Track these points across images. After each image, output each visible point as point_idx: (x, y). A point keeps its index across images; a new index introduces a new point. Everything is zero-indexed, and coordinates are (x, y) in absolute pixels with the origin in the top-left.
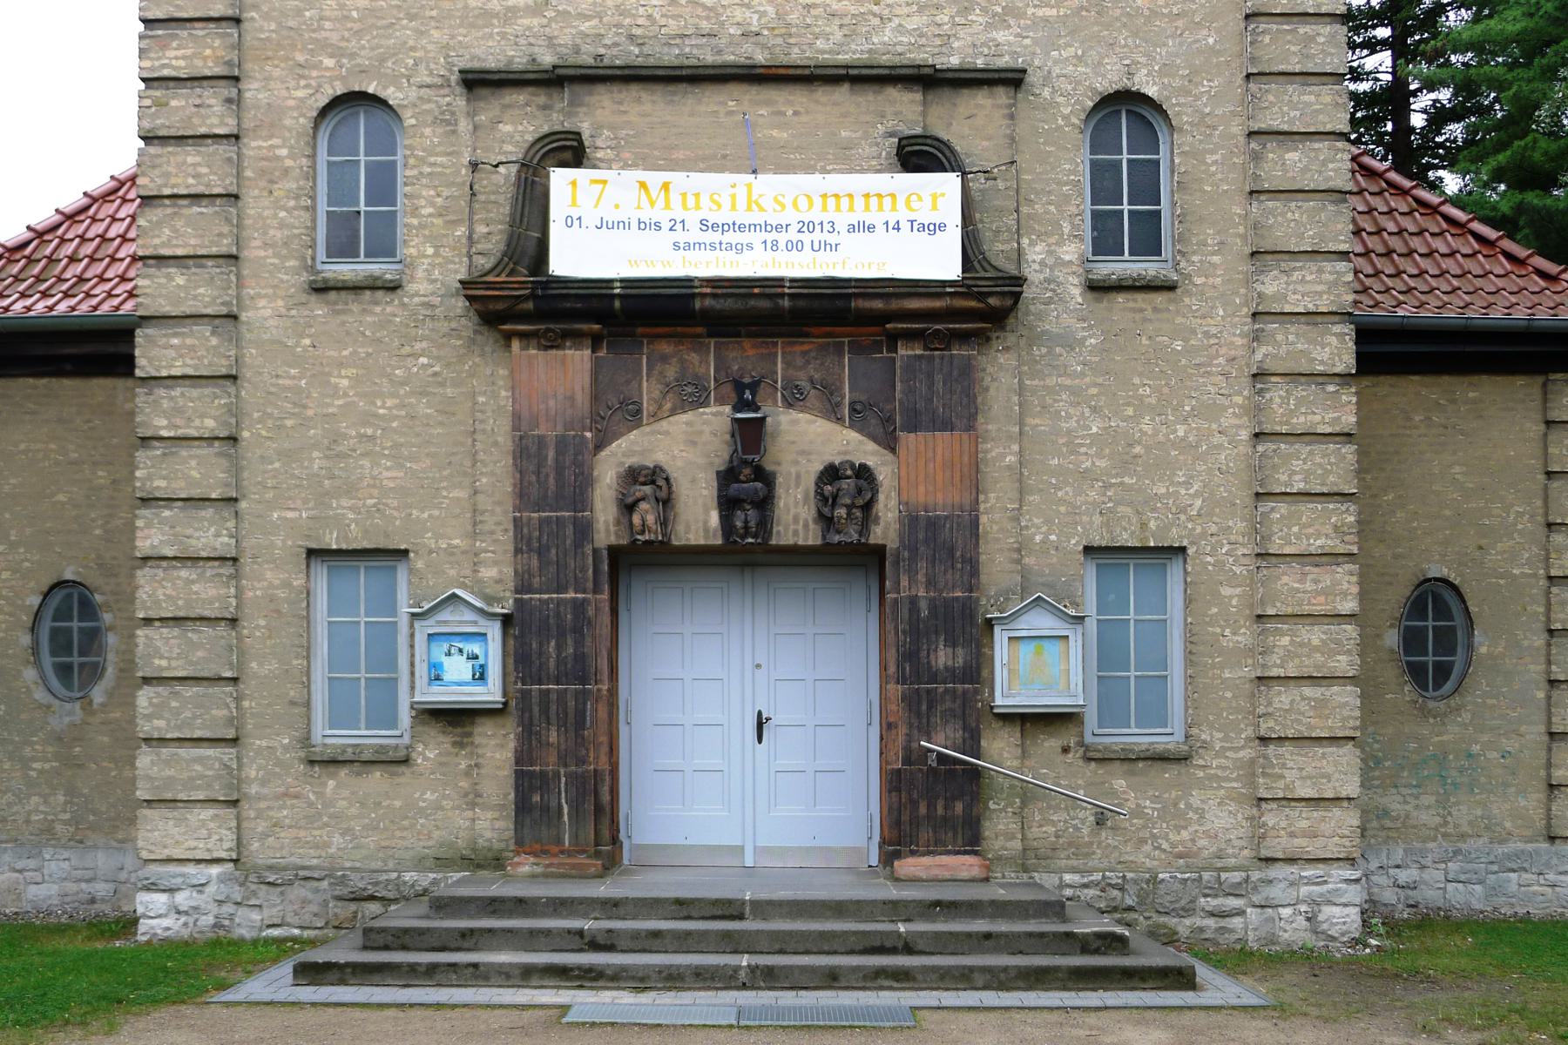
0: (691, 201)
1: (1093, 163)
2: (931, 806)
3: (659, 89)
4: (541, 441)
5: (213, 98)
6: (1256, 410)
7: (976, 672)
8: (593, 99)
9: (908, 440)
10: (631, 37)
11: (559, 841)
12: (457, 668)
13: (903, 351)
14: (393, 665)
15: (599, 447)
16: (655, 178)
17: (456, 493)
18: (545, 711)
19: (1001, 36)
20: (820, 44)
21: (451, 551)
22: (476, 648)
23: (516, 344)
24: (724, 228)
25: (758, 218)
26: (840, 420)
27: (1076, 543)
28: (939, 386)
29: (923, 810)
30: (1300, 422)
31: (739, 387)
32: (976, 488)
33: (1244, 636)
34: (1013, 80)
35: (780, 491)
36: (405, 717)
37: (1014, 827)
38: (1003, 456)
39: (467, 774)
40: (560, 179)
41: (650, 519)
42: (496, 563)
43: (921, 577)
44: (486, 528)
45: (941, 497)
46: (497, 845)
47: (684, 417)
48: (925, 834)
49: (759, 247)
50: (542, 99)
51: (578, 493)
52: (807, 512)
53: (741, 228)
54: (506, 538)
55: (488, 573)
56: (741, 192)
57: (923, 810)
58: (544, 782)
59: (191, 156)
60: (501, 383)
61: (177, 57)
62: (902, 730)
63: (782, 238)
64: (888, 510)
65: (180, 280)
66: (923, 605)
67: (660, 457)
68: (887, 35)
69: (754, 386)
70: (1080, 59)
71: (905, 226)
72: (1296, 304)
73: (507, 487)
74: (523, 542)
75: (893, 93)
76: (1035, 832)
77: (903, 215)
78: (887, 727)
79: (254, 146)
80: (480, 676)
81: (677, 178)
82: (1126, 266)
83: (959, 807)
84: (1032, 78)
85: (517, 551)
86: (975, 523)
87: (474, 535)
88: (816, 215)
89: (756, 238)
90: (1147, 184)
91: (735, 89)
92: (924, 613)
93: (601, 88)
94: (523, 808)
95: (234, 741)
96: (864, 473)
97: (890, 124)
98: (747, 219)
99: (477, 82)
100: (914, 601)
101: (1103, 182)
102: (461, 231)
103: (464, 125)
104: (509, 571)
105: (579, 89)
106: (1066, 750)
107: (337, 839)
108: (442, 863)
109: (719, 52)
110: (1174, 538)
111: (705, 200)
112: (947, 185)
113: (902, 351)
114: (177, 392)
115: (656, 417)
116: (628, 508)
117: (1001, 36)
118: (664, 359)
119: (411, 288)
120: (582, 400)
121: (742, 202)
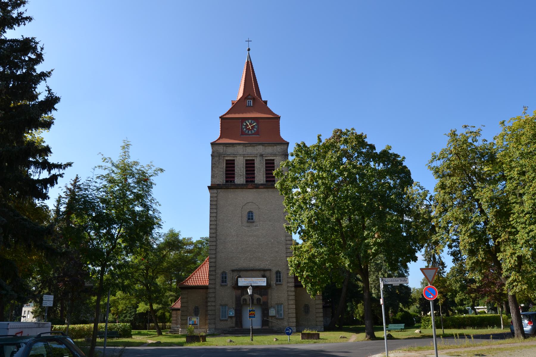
5: (214, 272)
6: (288, 294)
7: (268, 313)
9: (263, 296)
12: (231, 313)
13: (263, 290)
14: (226, 313)
16: (245, 278)
19: (269, 267)
30: (291, 294)
33: (287, 310)
34: (270, 270)
36: (227, 317)
40: (239, 279)
52: (256, 302)
59: (212, 276)
61: (212, 269)
64: (262, 301)
72: (290, 286)
79: (217, 275)
80: (233, 314)
82: (279, 283)
90: (280, 277)
94: (236, 323)
96: (260, 299)
99: (233, 271)
101: (277, 277)
103: (232, 274)
108: (230, 328)
110: (282, 303)
112: (265, 279)
116: (243, 302)
117: (269, 267)
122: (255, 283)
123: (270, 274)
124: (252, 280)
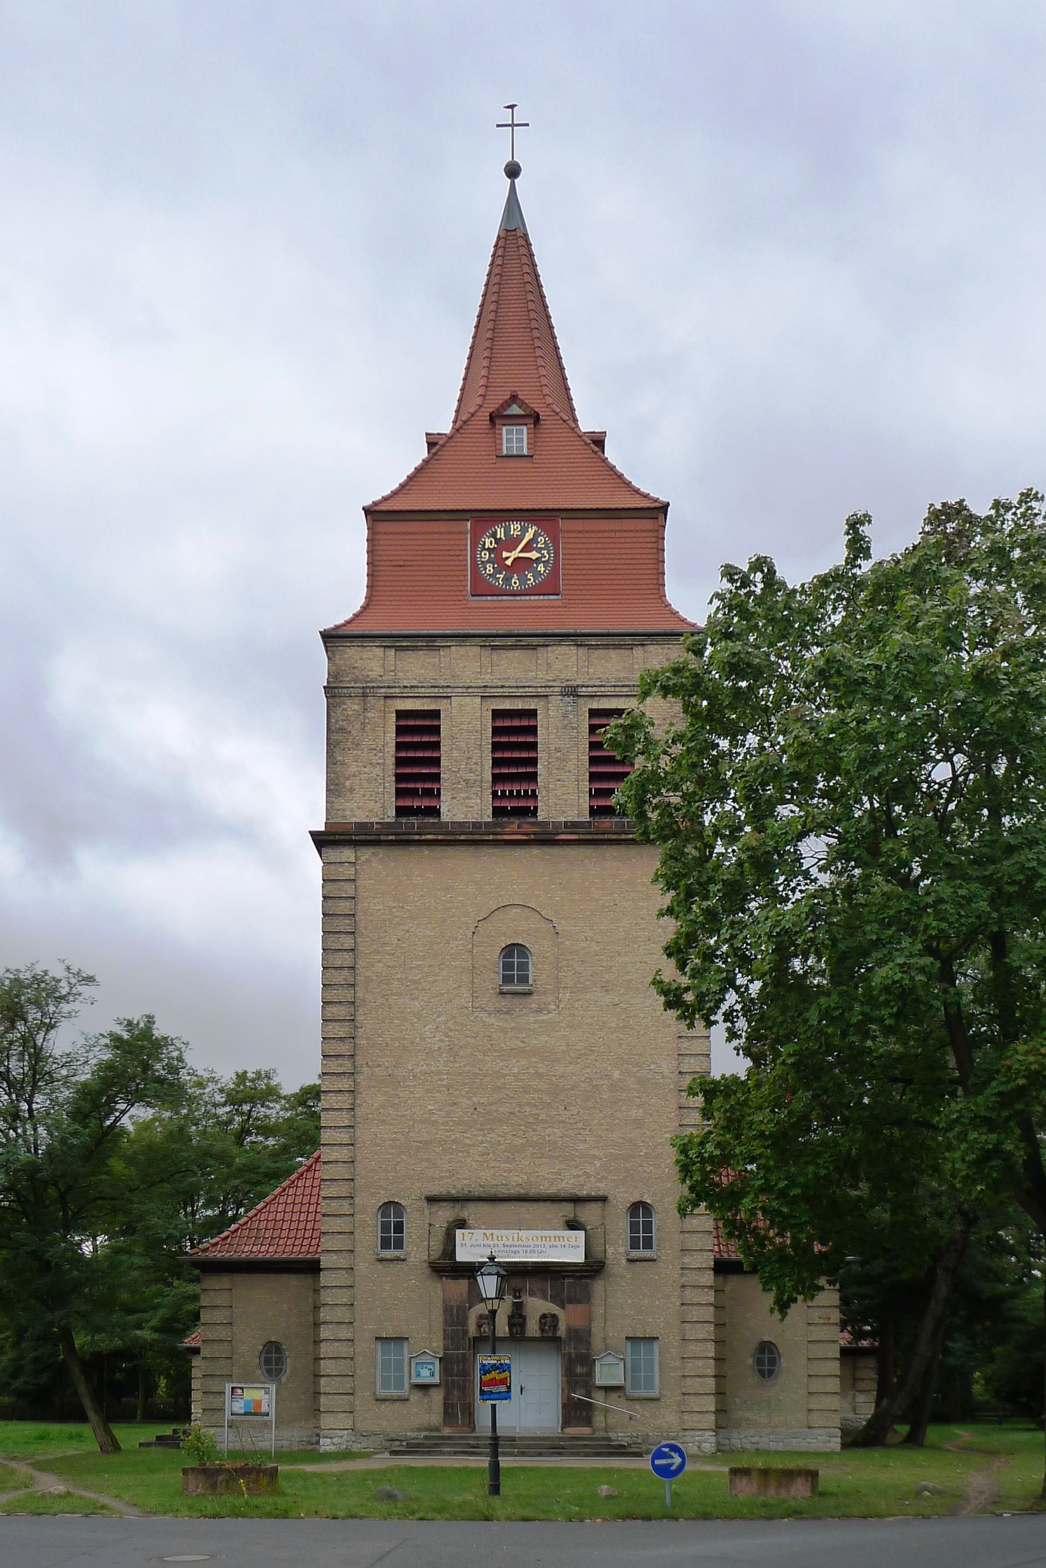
0: (500, 1239)
3: (489, 1203)
4: (452, 1307)
9: (569, 1306)
13: (567, 1281)
15: (470, 1308)
19: (599, 1185)
22: (431, 1367)
23: (444, 1279)
24: (510, 1246)
25: (521, 1243)
29: (573, 1414)
31: (515, 1291)
34: (603, 1199)
35: (528, 1321)
36: (406, 1386)
39: (428, 1404)
45: (578, 1323)
50: (452, 1205)
51: (463, 1321)
54: (441, 1334)
56: (516, 1236)
57: (573, 1414)
58: (452, 1406)
62: (566, 1391)
63: (528, 1249)
65: (335, 1257)
69: (519, 1291)
71: (567, 1246)
74: (446, 1336)
75: (565, 1204)
79: (358, 1217)
80: (433, 1375)
84: (610, 1198)
87: (430, 1333)
88: (539, 1242)
89: (521, 1249)
95: (352, 1394)
96: (554, 1317)
97: (564, 1213)
98: (518, 1243)
99: (431, 1200)
100: (570, 1354)
102: (426, 1243)
103: (427, 1212)
104: (441, 1344)
105: (464, 1203)
107: (385, 1422)
109: (509, 1190)
111: (504, 1238)
112: (581, 1234)
114: (334, 1290)
117: (599, 1185)
121: (516, 1239)
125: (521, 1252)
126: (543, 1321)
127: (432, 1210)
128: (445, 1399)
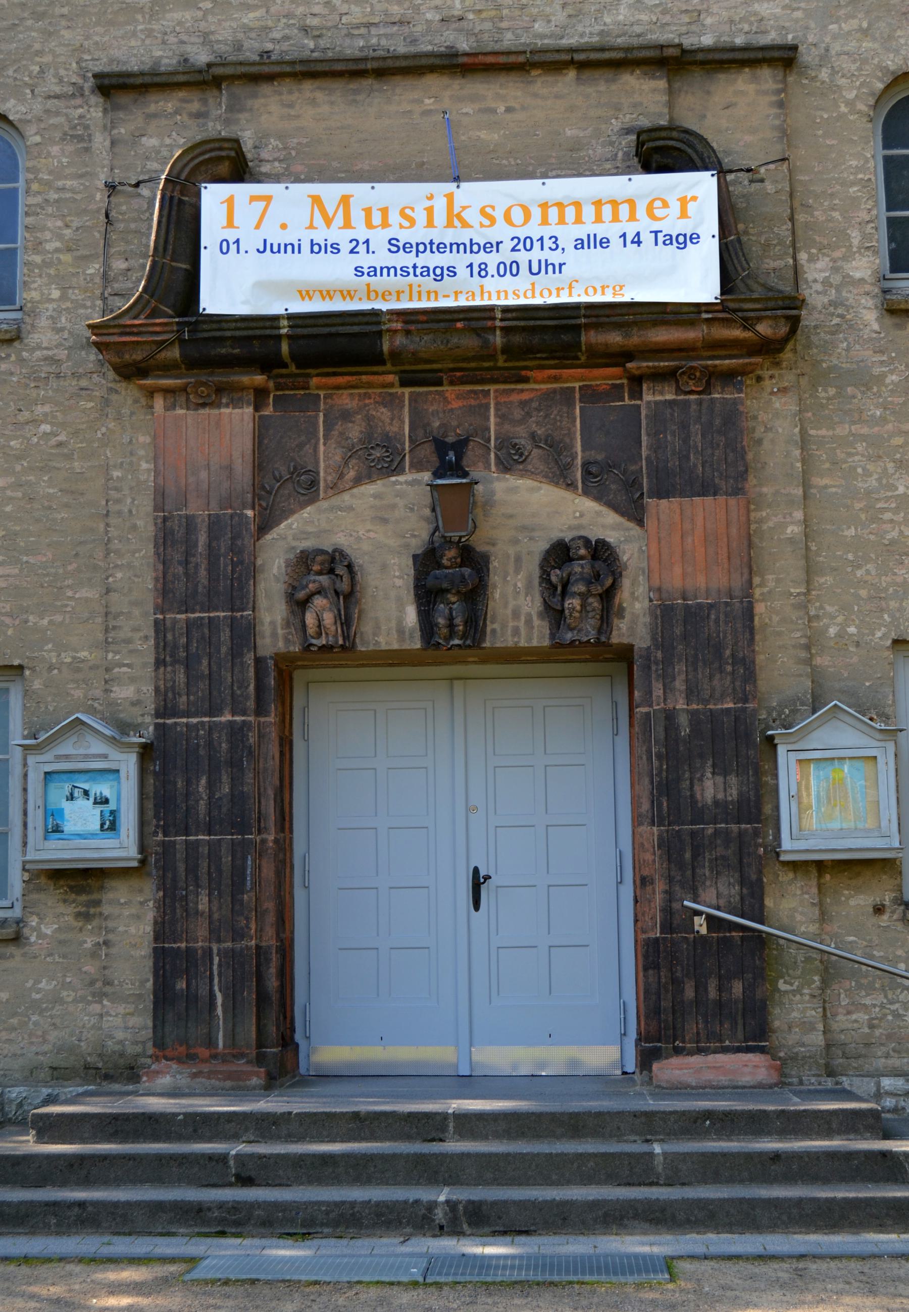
0: (377, 219)
1: (887, 160)
2: (701, 988)
3: (338, 85)
4: (190, 523)
8: (258, 103)
10: (305, 30)
11: (210, 1042)
15: (264, 528)
16: (331, 192)
17: (85, 593)
18: (192, 870)
20: (538, 27)
21: (76, 666)
22: (104, 789)
23: (159, 403)
24: (419, 248)
25: (464, 236)
26: (571, 486)
27: (881, 636)
28: (697, 439)
29: (689, 993)
31: (441, 447)
32: (750, 568)
35: (495, 578)
36: (16, 880)
37: (813, 1014)
38: (783, 526)
39: (94, 955)
41: (328, 618)
42: (133, 680)
43: (679, 684)
44: (121, 635)
46: (131, 1050)
47: (370, 489)
48: (691, 1027)
49: (463, 272)
50: (195, 106)
53: (441, 248)
54: (146, 648)
55: (124, 693)
56: (440, 205)
57: (689, 993)
60: (142, 453)
62: (660, 886)
63: (491, 260)
66: (683, 720)
67: (341, 540)
68: (623, 14)
69: (461, 446)
70: (865, 32)
71: (647, 238)
73: (148, 582)
76: (842, 1021)
77: (644, 225)
78: (643, 882)
80: (111, 825)
81: (359, 191)
83: (737, 988)
84: (807, 56)
85: (159, 663)
86: (749, 613)
88: (534, 230)
89: (460, 261)
91: (433, 81)
92: (685, 731)
93: (266, 89)
98: (449, 237)
100: (670, 716)
102: (94, 268)
103: (100, 141)
104: (148, 689)
105: (239, 89)
106: (879, 910)
109: (414, 41)
111: (394, 218)
113: (648, 397)
115: (335, 488)
118: (346, 416)
119: (33, 339)
120: (243, 469)
121: (440, 217)
122: (511, 269)
123: (785, 134)
124: (454, 218)
125: (463, 272)
126: (555, 576)
127: (122, 131)
128: (158, 936)
